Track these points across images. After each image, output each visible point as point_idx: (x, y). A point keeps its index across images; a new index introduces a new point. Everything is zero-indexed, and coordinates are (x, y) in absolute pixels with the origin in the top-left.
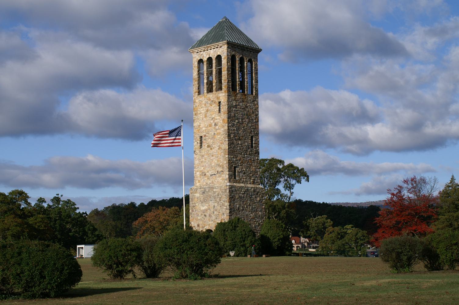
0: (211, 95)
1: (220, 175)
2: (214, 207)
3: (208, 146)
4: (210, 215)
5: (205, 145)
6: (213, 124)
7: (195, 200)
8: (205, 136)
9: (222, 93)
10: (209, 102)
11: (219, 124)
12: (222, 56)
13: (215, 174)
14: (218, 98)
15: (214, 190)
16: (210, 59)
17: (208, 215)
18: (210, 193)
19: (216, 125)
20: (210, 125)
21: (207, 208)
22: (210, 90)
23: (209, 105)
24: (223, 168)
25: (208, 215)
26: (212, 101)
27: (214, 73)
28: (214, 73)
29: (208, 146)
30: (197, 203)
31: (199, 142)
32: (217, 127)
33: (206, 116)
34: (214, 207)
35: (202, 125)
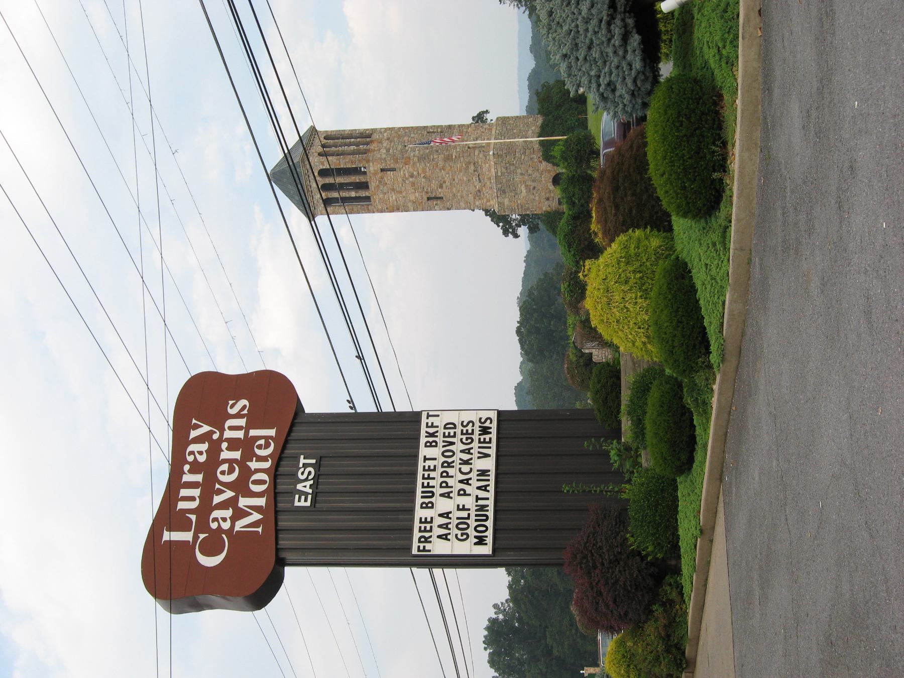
0: (372, 185)
2: (522, 174)
3: (441, 187)
4: (534, 181)
5: (440, 192)
6: (411, 179)
8: (427, 193)
10: (381, 187)
11: (411, 170)
14: (375, 174)
15: (499, 174)
18: (504, 181)
19: (412, 176)
20: (413, 184)
22: (364, 186)
24: (470, 163)
26: (380, 182)
29: (441, 187)
32: (415, 173)
33: (401, 192)
34: (522, 174)
35: (412, 197)
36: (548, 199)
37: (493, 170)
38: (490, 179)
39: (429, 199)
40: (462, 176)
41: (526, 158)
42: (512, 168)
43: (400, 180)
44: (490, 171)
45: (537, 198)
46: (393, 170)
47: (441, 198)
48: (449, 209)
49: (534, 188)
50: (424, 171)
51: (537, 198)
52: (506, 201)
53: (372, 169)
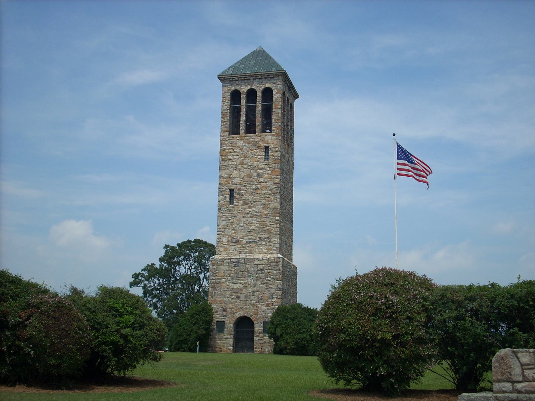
0: (251, 137)
1: (263, 243)
3: (244, 204)
4: (246, 297)
5: (238, 202)
6: (255, 174)
7: (220, 274)
8: (239, 189)
9: (272, 135)
10: (249, 146)
11: (266, 176)
12: (273, 89)
13: (255, 242)
14: (263, 140)
15: (256, 262)
16: (252, 94)
17: (242, 297)
18: (249, 266)
19: (259, 176)
20: (250, 177)
21: (241, 286)
22: (251, 129)
23: (248, 149)
24: (270, 233)
25: (242, 297)
26: (254, 145)
27: (259, 109)
28: (259, 109)
29: (244, 204)
30: (224, 278)
31: (228, 196)
32: (262, 179)
33: (242, 163)
34: (255, 286)
35: (234, 174)
36: (225, 310)
37: (260, 256)
38: (251, 252)
39: (232, 191)
40: (255, 224)
41: (272, 291)
42: (262, 276)
43: (255, 164)
44: (260, 253)
45: (226, 299)
46: (266, 158)
47: (231, 202)
48: (219, 210)
49: (238, 297)
50: (265, 188)
51: (226, 299)
52: (225, 267)
53: (269, 138)
